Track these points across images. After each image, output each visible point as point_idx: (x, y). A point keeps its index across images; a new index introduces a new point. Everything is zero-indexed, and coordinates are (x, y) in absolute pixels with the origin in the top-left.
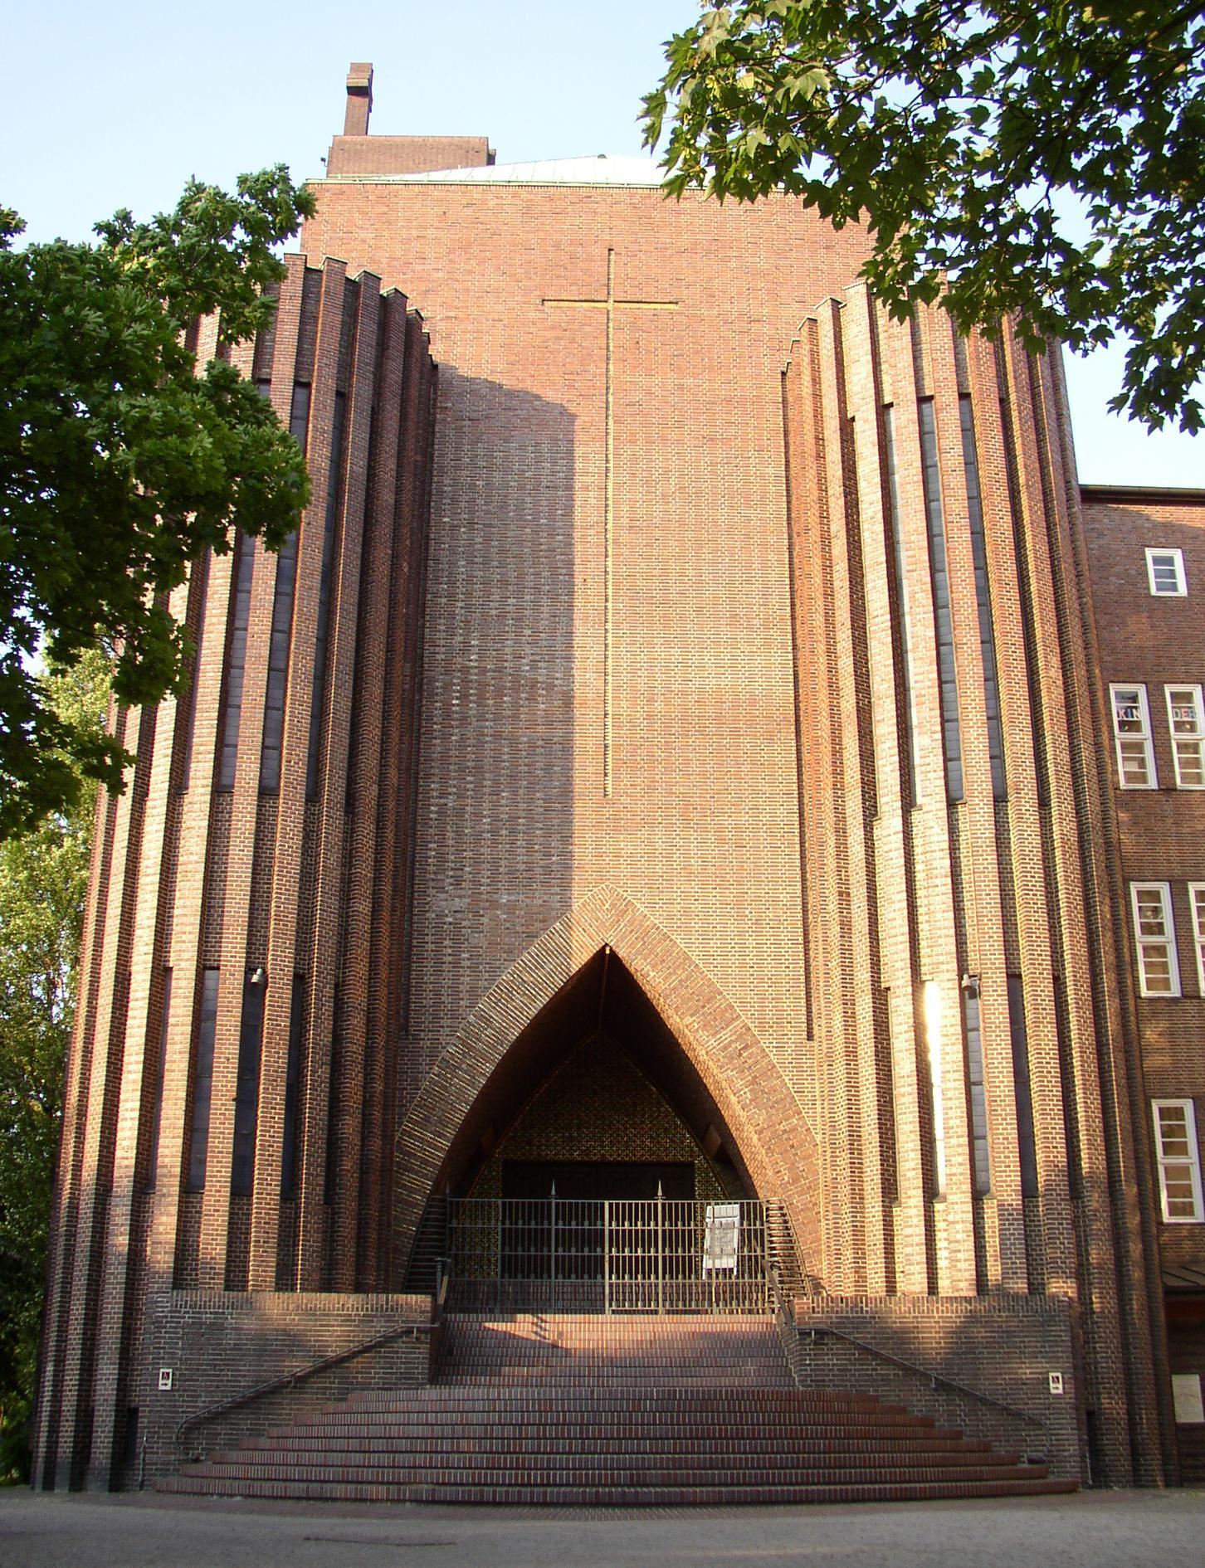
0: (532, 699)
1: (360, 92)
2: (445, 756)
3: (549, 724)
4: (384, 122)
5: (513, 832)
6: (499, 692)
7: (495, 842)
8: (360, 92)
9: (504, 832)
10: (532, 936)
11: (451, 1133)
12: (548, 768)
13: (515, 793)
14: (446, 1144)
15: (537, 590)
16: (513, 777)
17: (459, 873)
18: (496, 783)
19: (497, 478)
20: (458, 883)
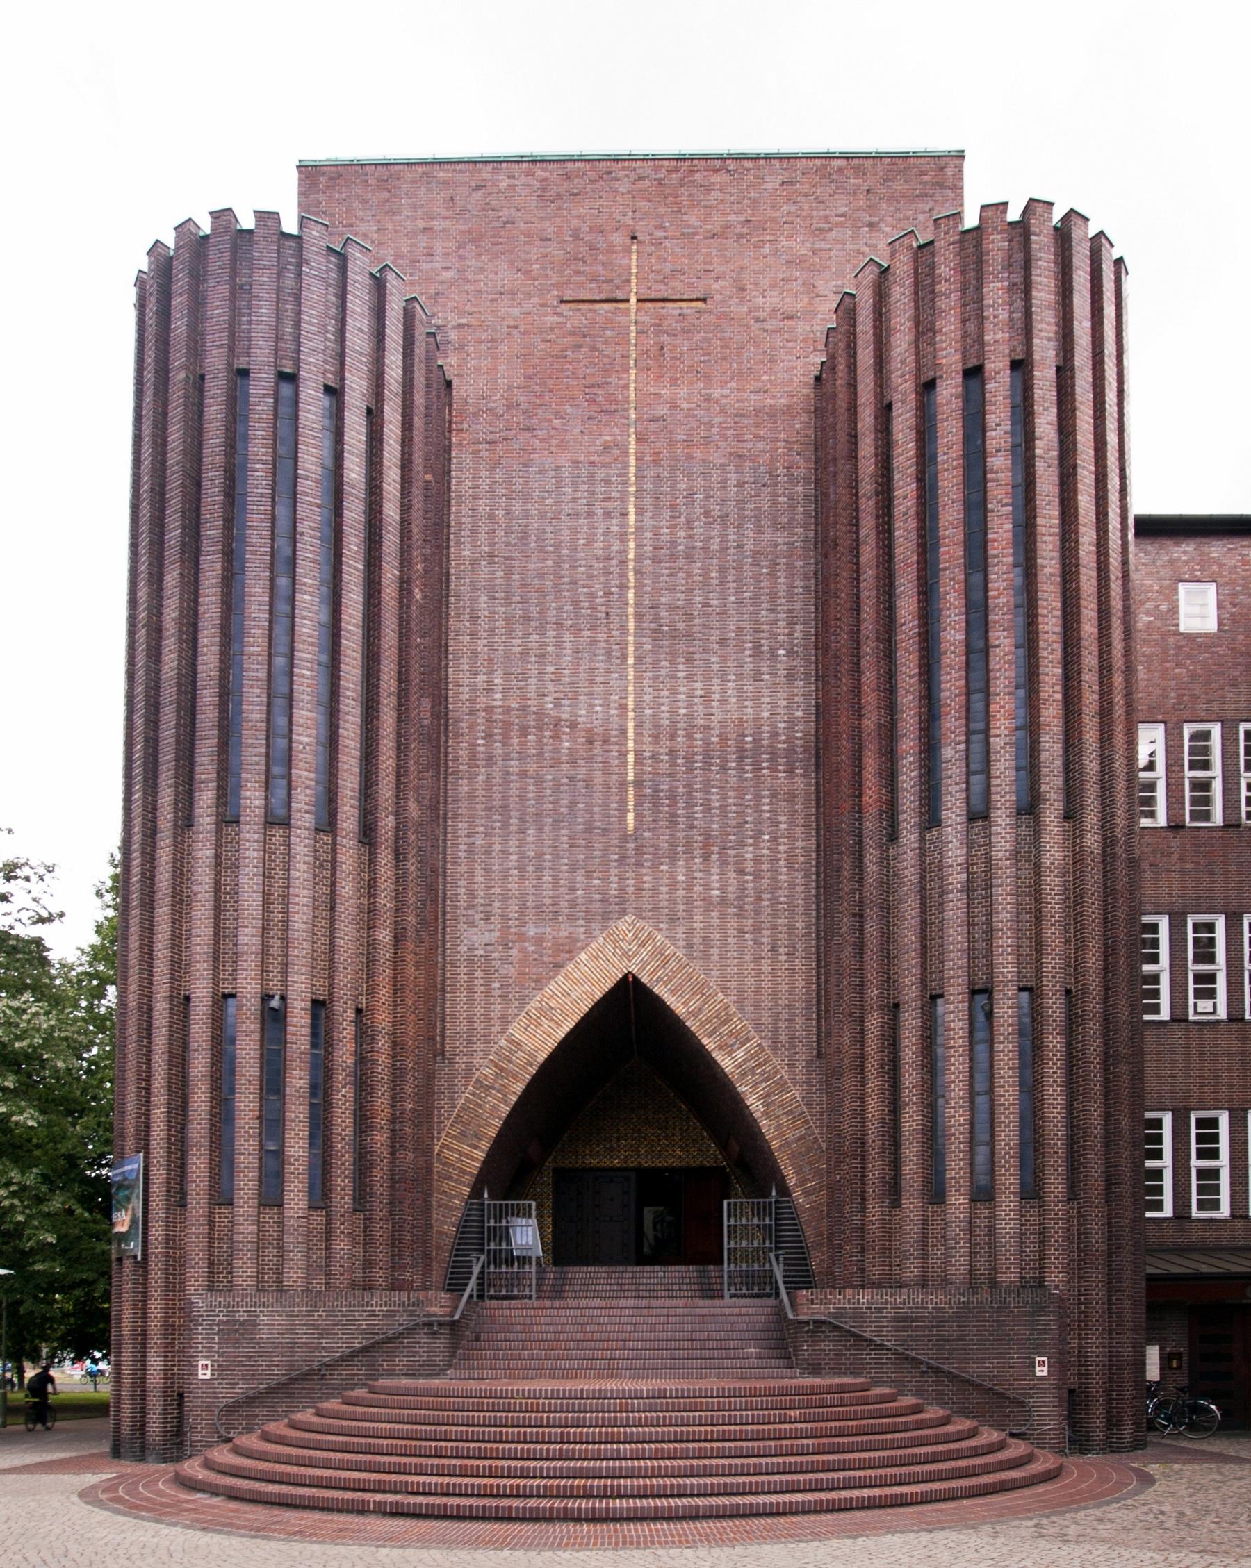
0: (556, 737)
2: (471, 796)
3: (573, 762)
5: (539, 868)
6: (524, 732)
7: (522, 878)
10: (558, 966)
11: (485, 1145)
12: (573, 804)
13: (540, 830)
14: (481, 1155)
15: (559, 625)
16: (538, 815)
17: (488, 908)
19: (517, 507)
20: (487, 919)
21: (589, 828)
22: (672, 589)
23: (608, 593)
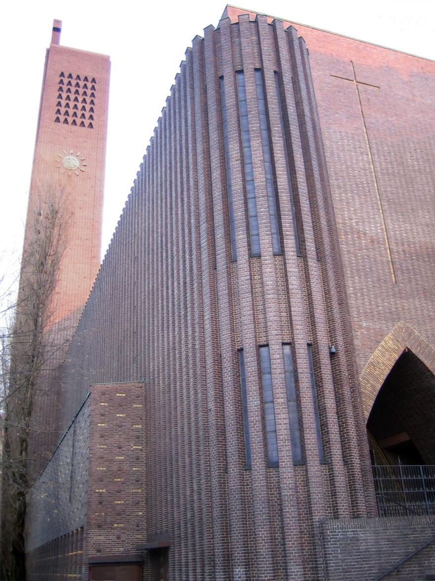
1: (57, 30)
4: (65, 41)
8: (57, 30)
9: (359, 294)
10: (378, 342)
12: (371, 268)
13: (360, 277)
15: (352, 192)
18: (352, 272)
21: (379, 280)
22: (391, 186)
23: (368, 183)
